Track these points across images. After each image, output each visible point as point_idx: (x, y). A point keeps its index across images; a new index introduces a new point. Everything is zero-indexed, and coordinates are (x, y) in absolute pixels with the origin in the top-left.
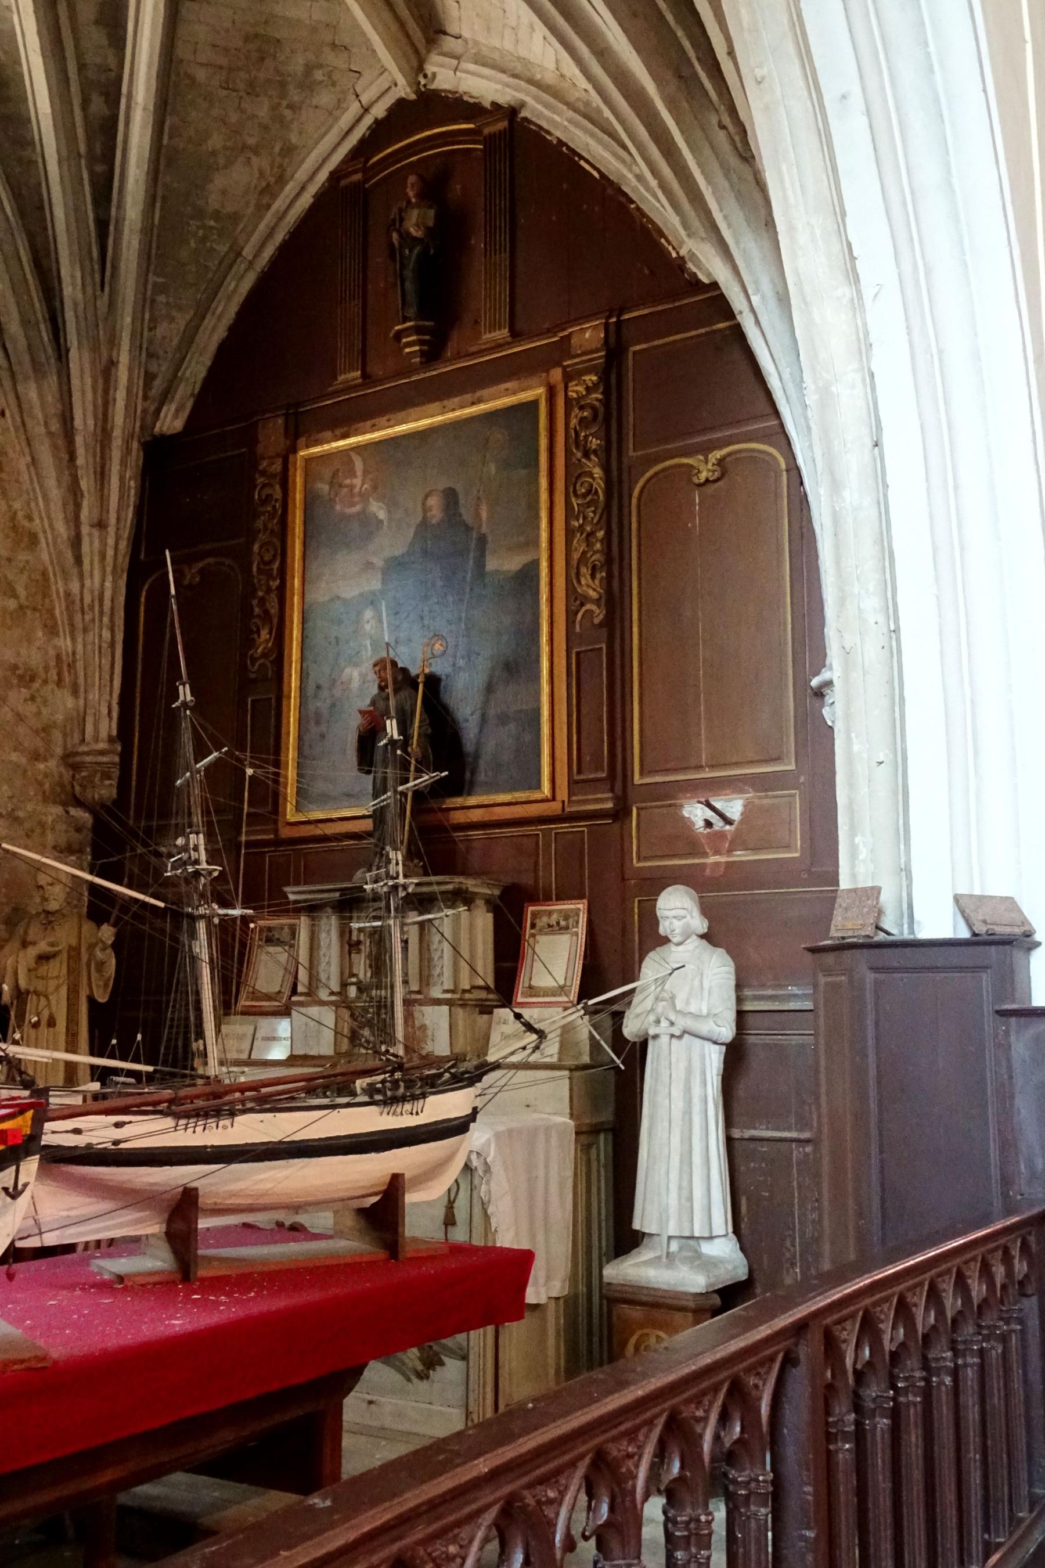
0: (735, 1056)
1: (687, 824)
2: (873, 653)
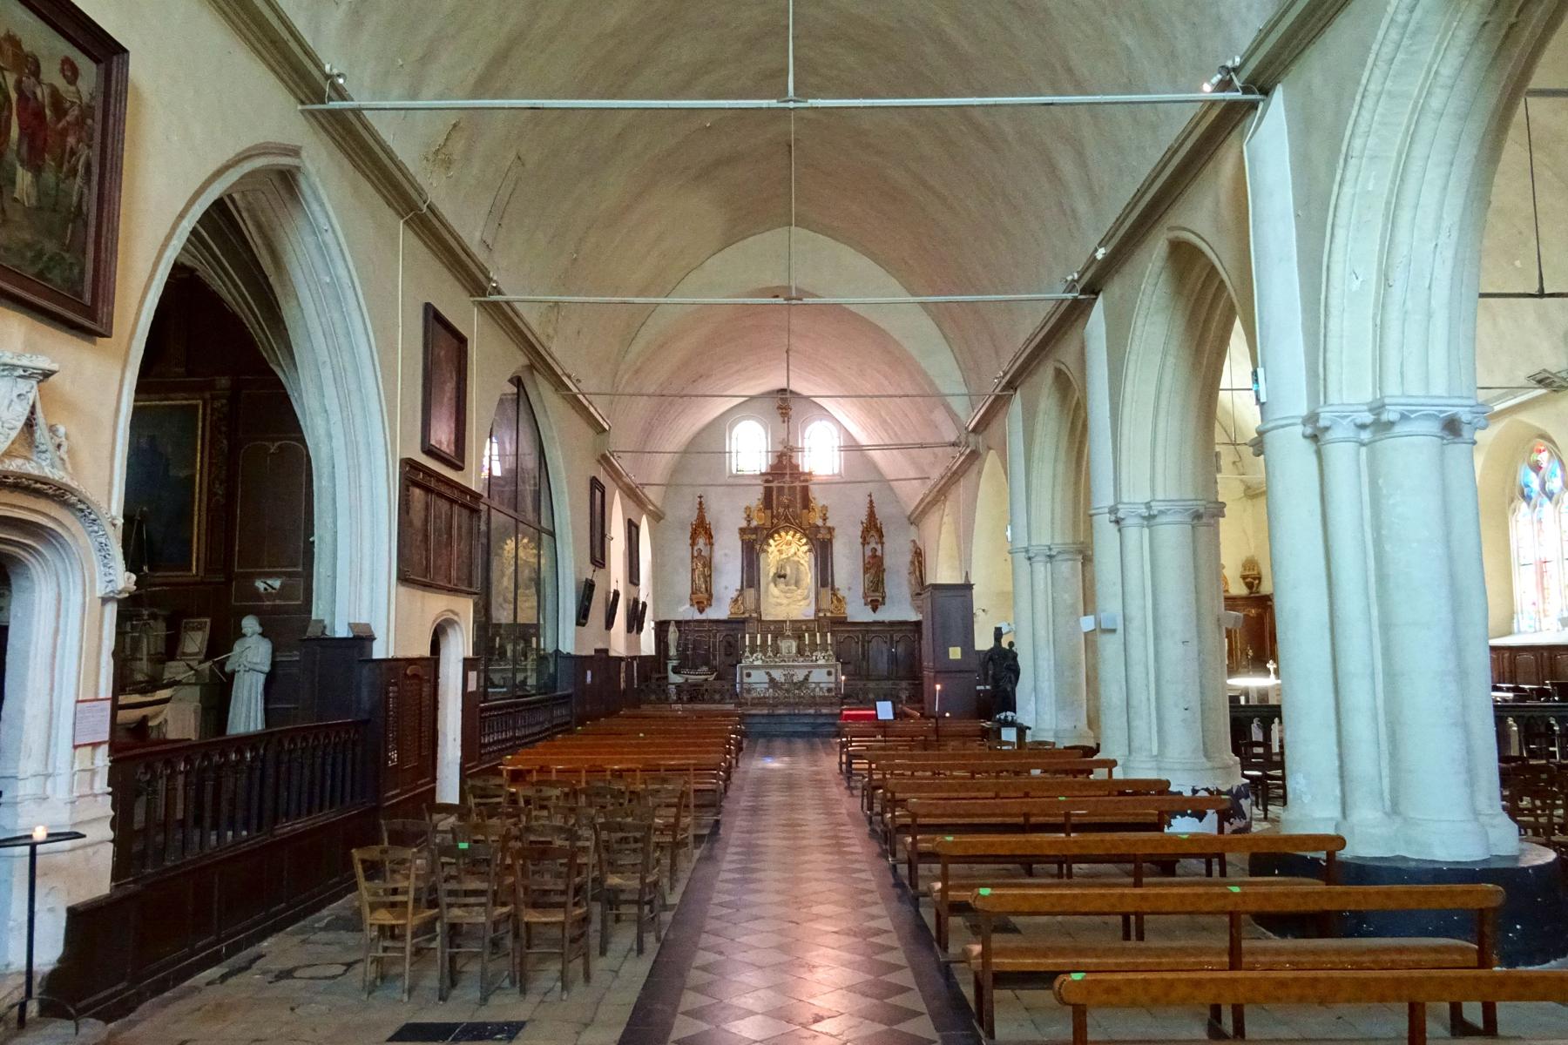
0: (271, 679)
1: (257, 589)
2: (328, 538)
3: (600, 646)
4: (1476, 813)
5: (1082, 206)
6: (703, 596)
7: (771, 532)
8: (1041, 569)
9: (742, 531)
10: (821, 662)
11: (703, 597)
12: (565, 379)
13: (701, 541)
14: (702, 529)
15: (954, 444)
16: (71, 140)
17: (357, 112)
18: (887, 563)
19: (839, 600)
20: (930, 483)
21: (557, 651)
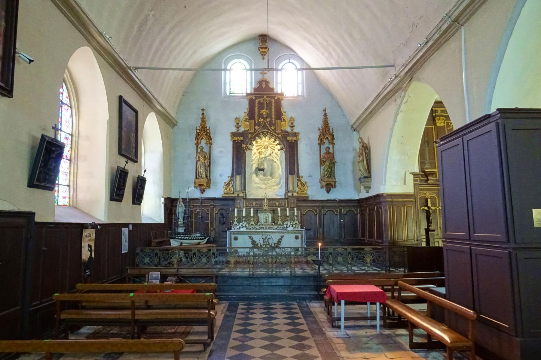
6: (203, 180)
7: (255, 135)
9: (233, 135)
10: (290, 229)
13: (203, 143)
14: (204, 133)
18: (337, 157)
19: (303, 184)
20: (392, 72)
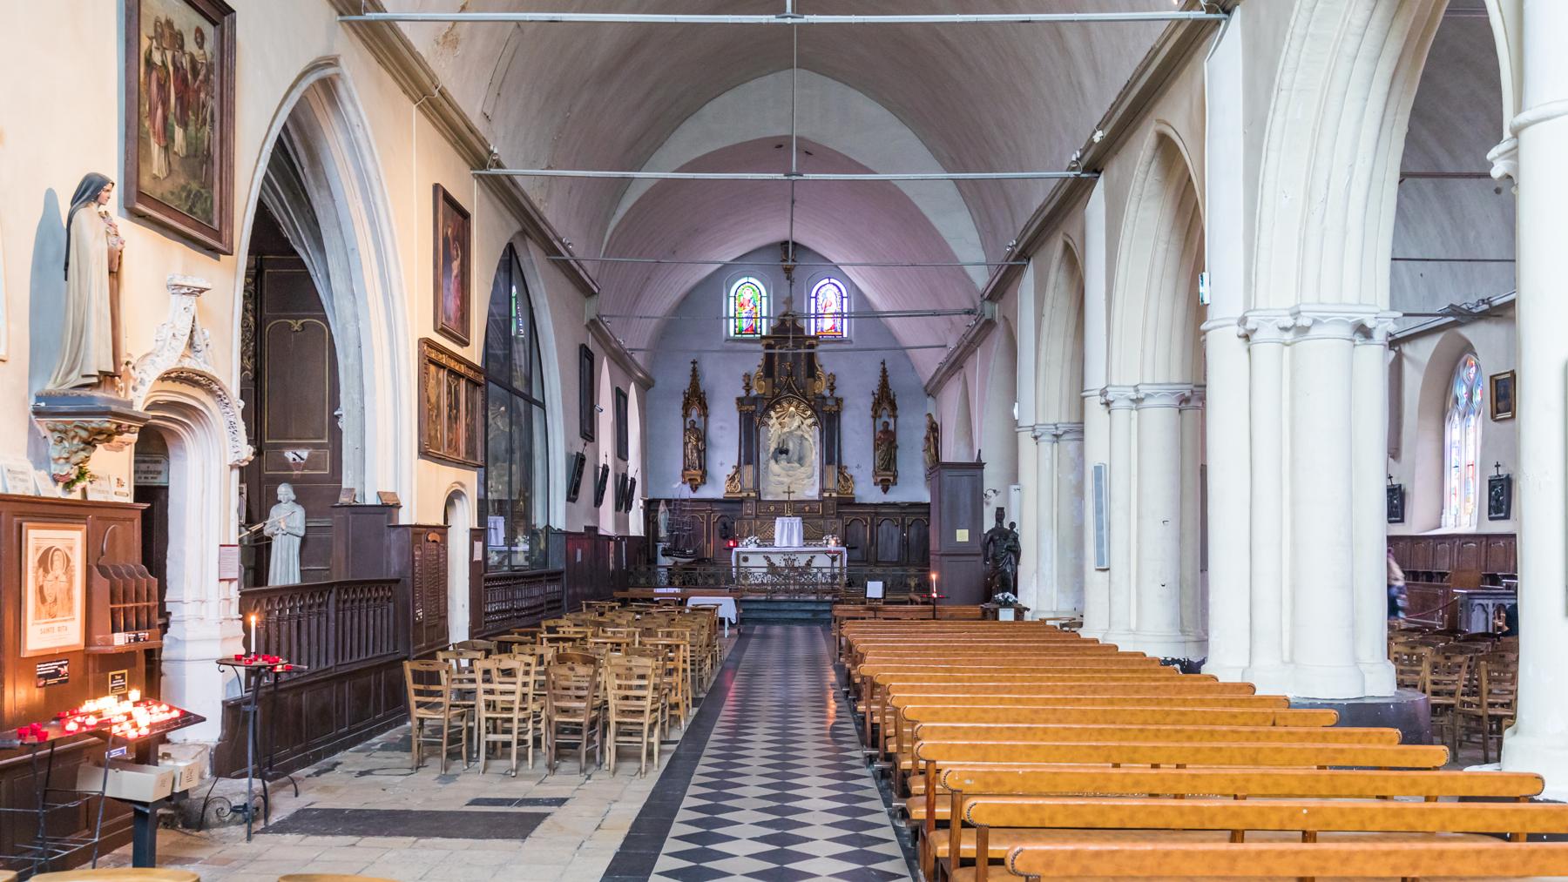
3: (590, 523)
4: (1356, 662)
5: (1088, 82)
8: (1046, 446)
9: (740, 401)
11: (698, 471)
12: (556, 243)
13: (694, 413)
14: (696, 398)
15: (969, 312)
16: (202, 95)
17: (390, 23)
18: (901, 438)
19: (846, 480)
21: (548, 526)
